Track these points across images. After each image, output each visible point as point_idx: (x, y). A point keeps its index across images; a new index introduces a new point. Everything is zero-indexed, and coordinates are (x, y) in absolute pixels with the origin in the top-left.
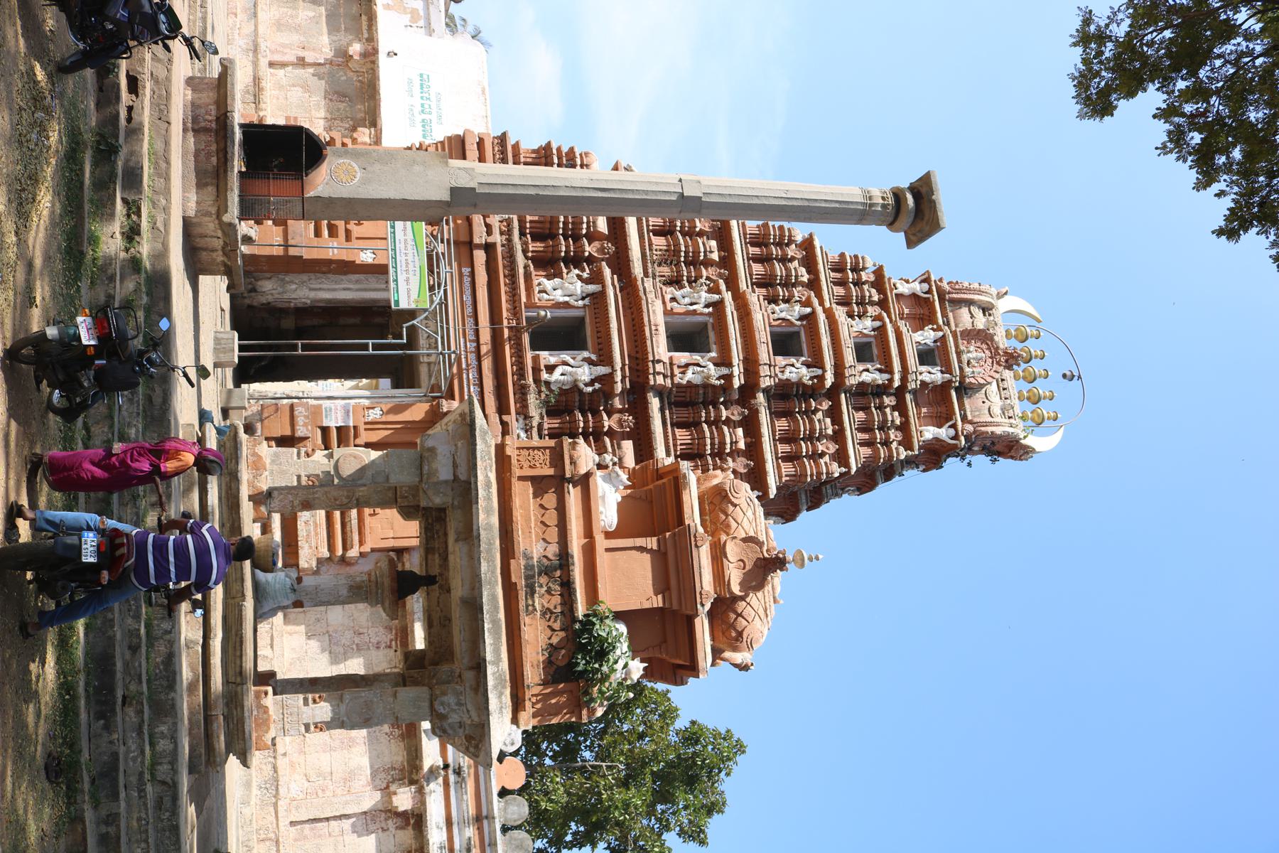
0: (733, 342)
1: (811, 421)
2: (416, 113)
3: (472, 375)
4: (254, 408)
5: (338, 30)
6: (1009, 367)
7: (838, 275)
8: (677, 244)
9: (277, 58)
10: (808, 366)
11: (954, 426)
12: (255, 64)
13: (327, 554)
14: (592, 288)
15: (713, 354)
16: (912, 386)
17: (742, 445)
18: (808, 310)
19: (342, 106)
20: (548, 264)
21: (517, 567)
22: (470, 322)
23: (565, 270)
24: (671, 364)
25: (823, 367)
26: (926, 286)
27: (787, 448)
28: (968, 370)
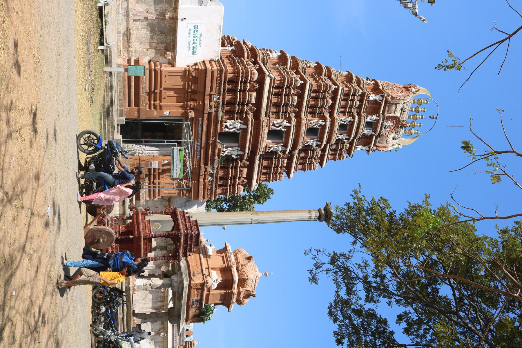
0: (290, 141)
1: (313, 153)
2: (191, 44)
3: (199, 152)
4: (128, 165)
5: (162, 3)
6: (401, 127)
7: (345, 98)
8: (281, 101)
9: (136, 18)
10: (317, 141)
11: (369, 147)
12: (128, 22)
13: (148, 198)
14: (244, 127)
15: (282, 144)
16: (358, 137)
17: (285, 165)
18: (324, 123)
19: (162, 37)
20: (230, 114)
21: (190, 303)
22: (200, 136)
23: (236, 116)
24: (266, 147)
25: (322, 143)
26: (381, 98)
27: (302, 161)
28: (383, 130)
